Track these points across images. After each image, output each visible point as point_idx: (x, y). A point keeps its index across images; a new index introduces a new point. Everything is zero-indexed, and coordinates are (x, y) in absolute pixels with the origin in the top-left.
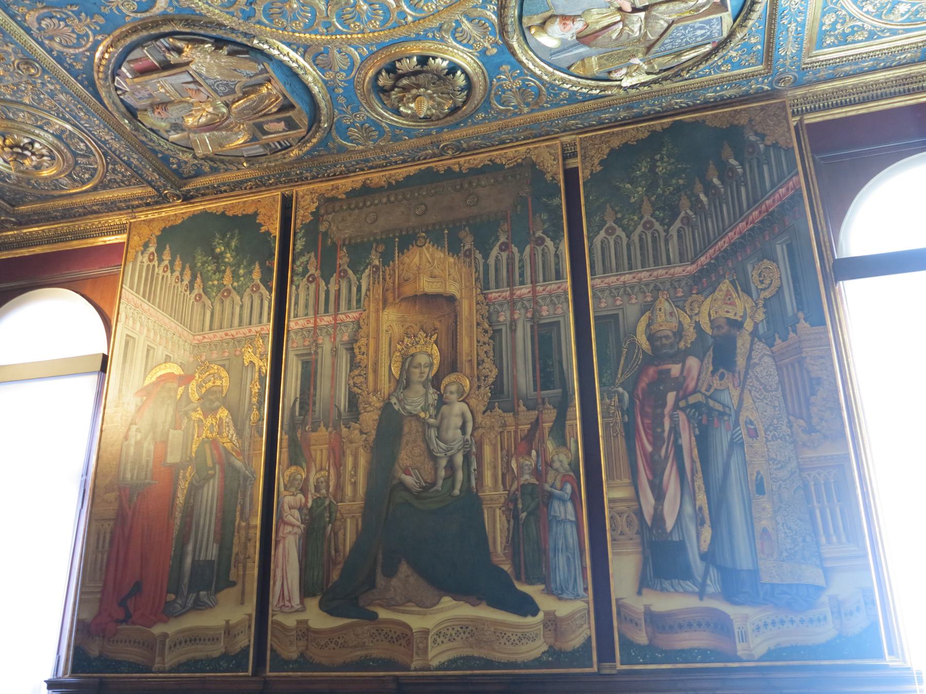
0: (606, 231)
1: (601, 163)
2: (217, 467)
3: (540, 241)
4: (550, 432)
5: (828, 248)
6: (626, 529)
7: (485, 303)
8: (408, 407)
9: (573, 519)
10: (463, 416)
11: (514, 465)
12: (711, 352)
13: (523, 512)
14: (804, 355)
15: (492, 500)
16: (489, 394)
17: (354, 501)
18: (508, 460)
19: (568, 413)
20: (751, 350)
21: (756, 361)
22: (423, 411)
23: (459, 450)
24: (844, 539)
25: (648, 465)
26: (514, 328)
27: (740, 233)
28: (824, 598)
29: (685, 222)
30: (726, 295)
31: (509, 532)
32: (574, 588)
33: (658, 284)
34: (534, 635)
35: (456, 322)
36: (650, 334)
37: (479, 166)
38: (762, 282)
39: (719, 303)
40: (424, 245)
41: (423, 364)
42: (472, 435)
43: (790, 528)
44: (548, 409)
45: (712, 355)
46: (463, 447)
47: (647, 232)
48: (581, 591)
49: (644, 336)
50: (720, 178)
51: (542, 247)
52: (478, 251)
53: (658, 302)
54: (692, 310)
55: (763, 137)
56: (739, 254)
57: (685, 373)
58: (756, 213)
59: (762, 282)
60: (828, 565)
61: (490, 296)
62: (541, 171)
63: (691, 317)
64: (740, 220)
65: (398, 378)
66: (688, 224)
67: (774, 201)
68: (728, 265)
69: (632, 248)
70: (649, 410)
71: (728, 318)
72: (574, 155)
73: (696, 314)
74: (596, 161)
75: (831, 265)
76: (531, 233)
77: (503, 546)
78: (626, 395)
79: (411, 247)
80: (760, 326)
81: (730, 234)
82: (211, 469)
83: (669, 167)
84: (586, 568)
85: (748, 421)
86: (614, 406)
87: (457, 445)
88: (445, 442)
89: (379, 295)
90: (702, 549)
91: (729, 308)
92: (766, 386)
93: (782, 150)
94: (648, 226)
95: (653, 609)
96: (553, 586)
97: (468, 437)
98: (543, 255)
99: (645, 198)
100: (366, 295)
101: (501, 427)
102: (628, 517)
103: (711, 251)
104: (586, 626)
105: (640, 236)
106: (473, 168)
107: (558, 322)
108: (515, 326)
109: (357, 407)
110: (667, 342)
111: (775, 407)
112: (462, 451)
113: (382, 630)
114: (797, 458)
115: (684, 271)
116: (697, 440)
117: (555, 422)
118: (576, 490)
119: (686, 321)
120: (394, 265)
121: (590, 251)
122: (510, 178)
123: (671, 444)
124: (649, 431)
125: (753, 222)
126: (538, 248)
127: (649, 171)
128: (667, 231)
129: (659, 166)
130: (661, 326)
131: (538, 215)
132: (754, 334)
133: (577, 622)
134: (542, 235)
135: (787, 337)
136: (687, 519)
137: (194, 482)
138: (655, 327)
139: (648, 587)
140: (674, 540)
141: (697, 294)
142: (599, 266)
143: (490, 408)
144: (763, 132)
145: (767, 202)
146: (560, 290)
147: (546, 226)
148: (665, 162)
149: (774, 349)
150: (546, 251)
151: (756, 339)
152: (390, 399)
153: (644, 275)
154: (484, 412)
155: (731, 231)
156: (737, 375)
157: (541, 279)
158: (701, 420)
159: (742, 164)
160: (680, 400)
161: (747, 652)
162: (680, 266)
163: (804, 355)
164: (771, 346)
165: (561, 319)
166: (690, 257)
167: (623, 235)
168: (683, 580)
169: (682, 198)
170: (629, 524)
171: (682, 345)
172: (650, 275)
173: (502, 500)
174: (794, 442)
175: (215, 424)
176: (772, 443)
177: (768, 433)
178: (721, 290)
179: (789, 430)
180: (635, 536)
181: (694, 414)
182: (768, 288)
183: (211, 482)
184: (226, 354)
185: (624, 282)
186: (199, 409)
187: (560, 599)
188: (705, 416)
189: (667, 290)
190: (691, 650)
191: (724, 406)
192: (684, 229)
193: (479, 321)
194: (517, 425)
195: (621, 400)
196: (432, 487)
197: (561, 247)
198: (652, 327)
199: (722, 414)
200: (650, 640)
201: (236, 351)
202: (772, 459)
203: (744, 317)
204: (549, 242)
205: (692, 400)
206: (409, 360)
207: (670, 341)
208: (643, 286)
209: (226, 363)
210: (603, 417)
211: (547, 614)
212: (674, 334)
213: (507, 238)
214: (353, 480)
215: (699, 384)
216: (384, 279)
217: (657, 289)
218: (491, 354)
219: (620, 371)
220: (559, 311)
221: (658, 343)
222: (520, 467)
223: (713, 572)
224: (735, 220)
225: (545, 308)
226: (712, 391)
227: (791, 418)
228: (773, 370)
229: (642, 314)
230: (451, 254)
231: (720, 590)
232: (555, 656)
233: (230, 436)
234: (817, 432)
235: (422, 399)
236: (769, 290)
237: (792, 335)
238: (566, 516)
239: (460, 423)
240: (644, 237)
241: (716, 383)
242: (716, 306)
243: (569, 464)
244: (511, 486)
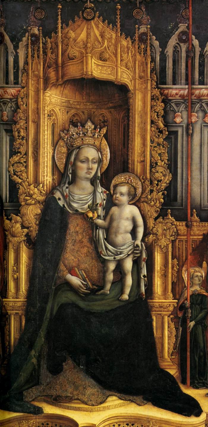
8: (75, 205)
10: (134, 221)
13: (191, 321)
15: (161, 307)
16: (162, 200)
17: (17, 298)
18: (178, 269)
22: (91, 210)
23: (129, 255)
26: (191, 132)
31: (176, 339)
35: (128, 116)
40: (93, 19)
41: (90, 158)
42: (143, 240)
46: (133, 253)
52: (154, 37)
61: (166, 92)
65: (62, 171)
77: (171, 352)
79: (76, 18)
87: (126, 249)
88: (114, 245)
89: (38, 71)
97: (138, 242)
100: (24, 69)
108: (193, 130)
109: (18, 198)
112: (131, 256)
113: (48, 424)
120: (57, 37)
143: (162, 214)
152: (53, 194)
154: (156, 219)
173: (171, 309)
193: (153, 119)
196: (100, 290)
206: (74, 153)
214: (16, 276)
216: (45, 53)
218: (166, 157)
222: (191, 278)
230: (124, 36)
235: (90, 197)
239: (130, 227)
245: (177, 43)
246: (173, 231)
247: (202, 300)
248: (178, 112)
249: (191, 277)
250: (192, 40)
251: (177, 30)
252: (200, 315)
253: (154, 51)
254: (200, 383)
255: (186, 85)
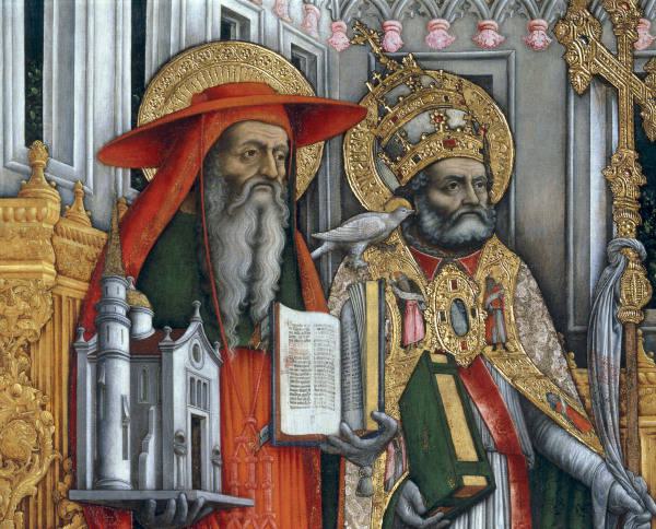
2: (498, 463)
82: (473, 468)
137: (407, 512)
175: (469, 303)
183: (479, 513)
184: (490, 38)
186: (396, 238)
201: (532, 29)
209: (496, 70)
233: (538, 355)
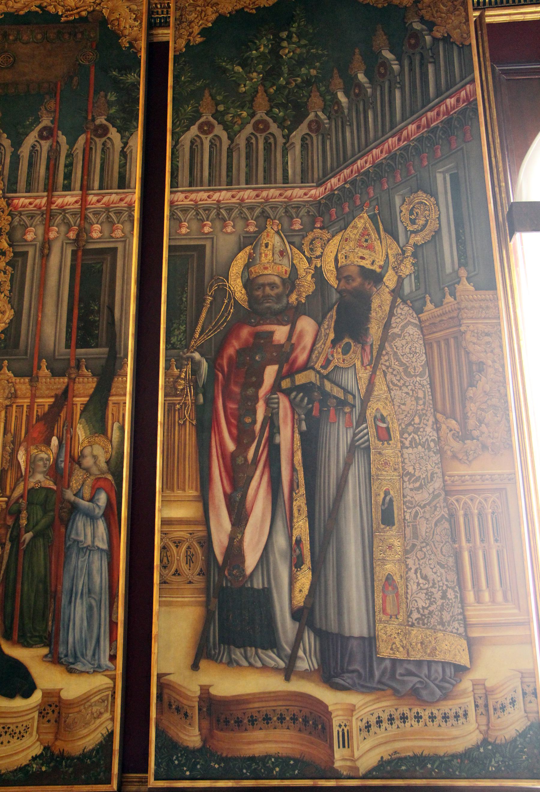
0: (200, 128)
1: (204, 32)
3: (103, 131)
4: (82, 412)
5: (503, 189)
6: (184, 567)
7: (7, 212)
9: (105, 546)
11: (21, 457)
12: (334, 312)
13: (27, 532)
14: (463, 328)
18: (13, 450)
19: (114, 385)
20: (391, 314)
21: (396, 330)
24: (499, 597)
25: (227, 471)
26: (46, 251)
27: (389, 151)
28: (466, 684)
29: (314, 126)
30: (363, 235)
32: (94, 655)
33: (267, 209)
34: (22, 729)
36: (248, 279)
37: (22, 13)
38: (413, 222)
39: (351, 244)
43: (425, 578)
44: (84, 376)
45: (335, 317)
47: (258, 135)
48: (105, 661)
49: (239, 280)
50: (366, 74)
51: (104, 139)
53: (265, 234)
54: (312, 250)
55: (431, 25)
56: (384, 180)
57: (294, 340)
58: (412, 127)
59: (413, 222)
60: (475, 633)
61: (16, 201)
62: (114, 32)
63: (309, 260)
64: (389, 135)
66: (317, 131)
67: (438, 114)
68: (368, 194)
69: (235, 155)
70: (236, 389)
71: (362, 267)
72: (166, 24)
73: (317, 257)
74: (196, 30)
75: (506, 213)
76: (90, 118)
78: (205, 365)
80: (406, 282)
81: (374, 151)
83: (298, 51)
84: (117, 624)
85: (379, 416)
86: (184, 379)
90: (295, 602)
91: (362, 252)
92: (407, 367)
93: (455, 48)
94: (261, 127)
95: (214, 691)
96: (61, 649)
98: (103, 150)
99: (260, 88)
101: (7, 398)
102: (189, 548)
103: (347, 172)
104: (107, 715)
105: (248, 140)
106: (13, 14)
107: (115, 250)
108: (49, 249)
110: (273, 293)
111: (417, 399)
114: (443, 475)
115: (305, 194)
116: (302, 441)
117: (92, 397)
118: (114, 502)
119: (303, 265)
121: (173, 153)
122: (67, 36)
123: (263, 442)
124: (233, 421)
125: (408, 138)
126: (97, 140)
127: (269, 53)
128: (287, 137)
129: (285, 48)
130: (266, 268)
131: (102, 93)
132: (397, 292)
133: (95, 709)
134: (105, 122)
135: (442, 302)
136: (277, 556)
138: (256, 270)
139: (210, 657)
140: (255, 586)
141: (321, 228)
142: (184, 175)
144: (432, 19)
145: (429, 114)
146: (122, 204)
147: (112, 111)
148: (294, 43)
149: (423, 316)
150: (109, 145)
151: (399, 300)
153: (248, 195)
155: (376, 147)
156: (368, 349)
157: (96, 184)
158: (311, 410)
159: (399, 59)
160: (284, 378)
161: (349, 763)
162: (301, 188)
163: (463, 328)
164: (419, 311)
165: (120, 246)
166: (316, 176)
167: (224, 136)
168: (264, 648)
169: (312, 95)
170: (190, 559)
171: (293, 298)
172: (257, 196)
174: (441, 452)
176: (410, 450)
177: (406, 435)
178: (355, 227)
179: (435, 434)
180: (197, 578)
181: (302, 399)
182: (421, 230)
185: (219, 201)
187: (71, 672)
188: (316, 404)
189: (279, 220)
190: (265, 759)
191: (346, 391)
192: (311, 138)
194: (33, 397)
195: (195, 371)
197: (130, 143)
198: (252, 269)
199: (342, 403)
200: (205, 741)
202: (408, 473)
203: (384, 267)
204: (114, 134)
205: (301, 379)
207: (276, 291)
208: (245, 210)
210: (166, 395)
211: (46, 694)
212: (283, 281)
213: (52, 122)
215: (314, 356)
217: (264, 216)
219: (199, 329)
220: (118, 234)
221: (259, 293)
222: (31, 462)
223: (309, 638)
224: (384, 133)
225: (97, 227)
226: (331, 368)
227: (439, 415)
228: (419, 347)
229: (240, 250)
231: (316, 667)
232: (52, 764)
234: (473, 439)
236: (423, 234)
237: (449, 299)
238: (93, 542)
240: (253, 141)
241: (338, 358)
242: (347, 248)
243: (108, 462)
244: (13, 490)
245: (37, 141)
246: (10, 392)
247: (47, 497)
248: (31, 226)
249: (32, 461)
250: (58, 136)
251: (38, 125)
252: (43, 521)
253: (3, 152)
254: (36, 636)
255: (44, 192)
